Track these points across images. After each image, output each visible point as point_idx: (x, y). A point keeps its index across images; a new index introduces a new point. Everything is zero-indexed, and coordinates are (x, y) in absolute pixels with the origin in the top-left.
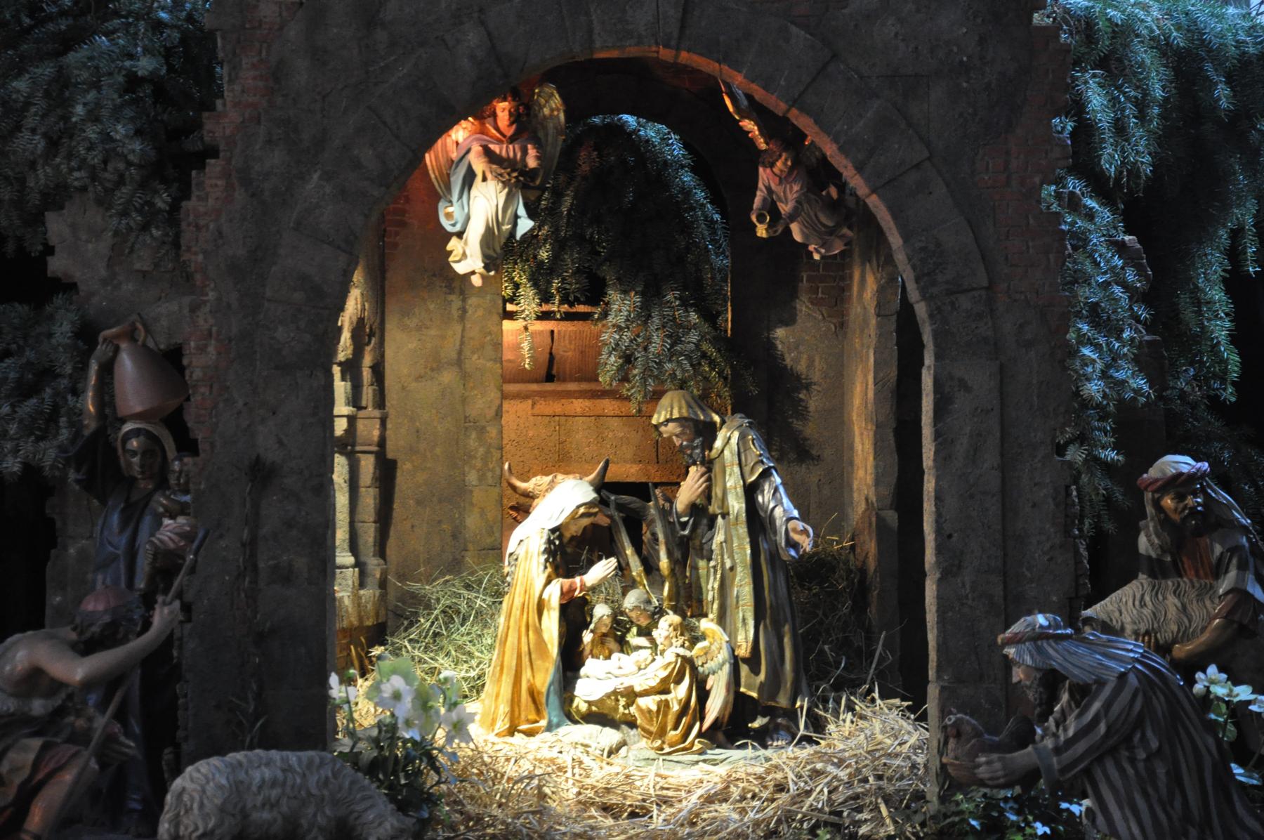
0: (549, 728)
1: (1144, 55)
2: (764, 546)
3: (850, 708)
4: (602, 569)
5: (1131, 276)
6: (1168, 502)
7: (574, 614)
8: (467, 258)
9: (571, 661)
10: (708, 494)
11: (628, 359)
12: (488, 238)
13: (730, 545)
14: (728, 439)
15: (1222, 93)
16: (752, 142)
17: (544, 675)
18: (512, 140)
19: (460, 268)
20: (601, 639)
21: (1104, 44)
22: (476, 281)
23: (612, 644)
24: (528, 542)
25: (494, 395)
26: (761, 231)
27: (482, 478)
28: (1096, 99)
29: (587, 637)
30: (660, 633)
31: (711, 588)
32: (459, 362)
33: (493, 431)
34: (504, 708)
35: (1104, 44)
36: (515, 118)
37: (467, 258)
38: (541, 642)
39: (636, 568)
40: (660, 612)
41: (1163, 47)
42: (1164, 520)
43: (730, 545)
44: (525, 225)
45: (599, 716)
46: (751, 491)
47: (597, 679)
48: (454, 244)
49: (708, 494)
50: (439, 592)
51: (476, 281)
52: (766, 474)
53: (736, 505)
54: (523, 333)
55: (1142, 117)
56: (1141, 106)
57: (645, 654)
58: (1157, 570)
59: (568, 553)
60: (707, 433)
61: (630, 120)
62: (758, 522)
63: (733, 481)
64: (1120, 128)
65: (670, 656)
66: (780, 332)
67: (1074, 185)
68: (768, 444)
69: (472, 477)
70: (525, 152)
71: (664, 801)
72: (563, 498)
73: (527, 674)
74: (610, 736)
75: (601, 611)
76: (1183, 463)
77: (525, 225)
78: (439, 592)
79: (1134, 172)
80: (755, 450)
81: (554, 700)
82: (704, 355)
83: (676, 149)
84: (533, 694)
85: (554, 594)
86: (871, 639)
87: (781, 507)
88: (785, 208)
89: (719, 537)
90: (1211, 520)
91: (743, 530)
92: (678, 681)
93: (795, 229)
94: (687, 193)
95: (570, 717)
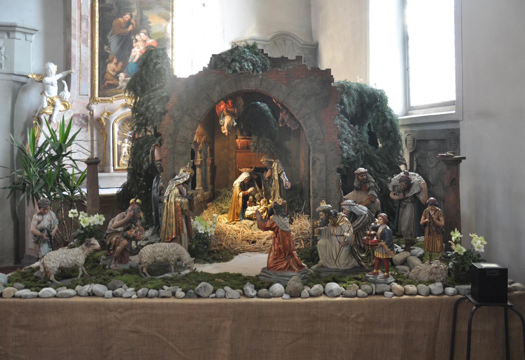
0: (240, 220)
1: (353, 92)
2: (282, 186)
3: (299, 216)
4: (250, 190)
5: (352, 132)
6: (360, 177)
7: (245, 198)
8: (225, 131)
9: (244, 207)
10: (271, 175)
11: (256, 148)
12: (228, 126)
13: (276, 185)
14: (275, 165)
15: (367, 99)
16: (279, 108)
17: (239, 211)
18: (232, 108)
19: (223, 132)
20: (251, 202)
21: (346, 90)
22: (226, 134)
23: (253, 204)
24: (237, 183)
25: (234, 154)
26: (280, 125)
27: (232, 169)
28: (345, 100)
29: (248, 202)
30: (262, 202)
31: (272, 193)
32: (228, 148)
33: (234, 160)
34: (232, 216)
35: (346, 90)
36: (232, 103)
37: (225, 131)
38: (239, 204)
39: (258, 189)
40: (262, 198)
41: (356, 90)
42: (359, 180)
43: (276, 185)
44: (235, 124)
45: (250, 218)
46: (279, 175)
47: (250, 211)
48: (222, 127)
49: (271, 175)
50: (223, 191)
51: (226, 134)
52: (282, 172)
53: (276, 178)
54: (240, 141)
55: (353, 103)
56: (353, 101)
57: (258, 206)
58: (358, 189)
59: (244, 186)
60: (271, 163)
61: (259, 103)
62: (280, 181)
63: (276, 173)
64: (349, 105)
65: (262, 207)
66: (287, 142)
67: (342, 116)
68: (283, 165)
69: (230, 169)
70: (234, 110)
71: (259, 239)
72: (244, 176)
73: (236, 210)
74: (251, 222)
75: (251, 197)
76: (362, 170)
77: (235, 124)
78: (223, 191)
79: (352, 113)
80: (280, 167)
81: (241, 215)
82: (271, 147)
83: (267, 108)
84: (237, 213)
85: (241, 194)
86: (303, 201)
87: (285, 178)
88: (286, 120)
89: (273, 184)
90: (367, 181)
91: (278, 183)
92: (264, 212)
93: (288, 124)
94: (269, 116)
95: (244, 218)
